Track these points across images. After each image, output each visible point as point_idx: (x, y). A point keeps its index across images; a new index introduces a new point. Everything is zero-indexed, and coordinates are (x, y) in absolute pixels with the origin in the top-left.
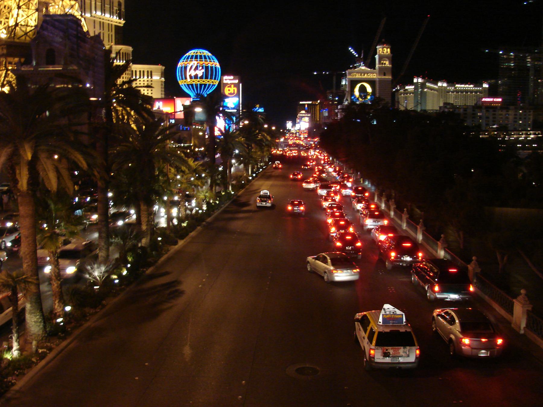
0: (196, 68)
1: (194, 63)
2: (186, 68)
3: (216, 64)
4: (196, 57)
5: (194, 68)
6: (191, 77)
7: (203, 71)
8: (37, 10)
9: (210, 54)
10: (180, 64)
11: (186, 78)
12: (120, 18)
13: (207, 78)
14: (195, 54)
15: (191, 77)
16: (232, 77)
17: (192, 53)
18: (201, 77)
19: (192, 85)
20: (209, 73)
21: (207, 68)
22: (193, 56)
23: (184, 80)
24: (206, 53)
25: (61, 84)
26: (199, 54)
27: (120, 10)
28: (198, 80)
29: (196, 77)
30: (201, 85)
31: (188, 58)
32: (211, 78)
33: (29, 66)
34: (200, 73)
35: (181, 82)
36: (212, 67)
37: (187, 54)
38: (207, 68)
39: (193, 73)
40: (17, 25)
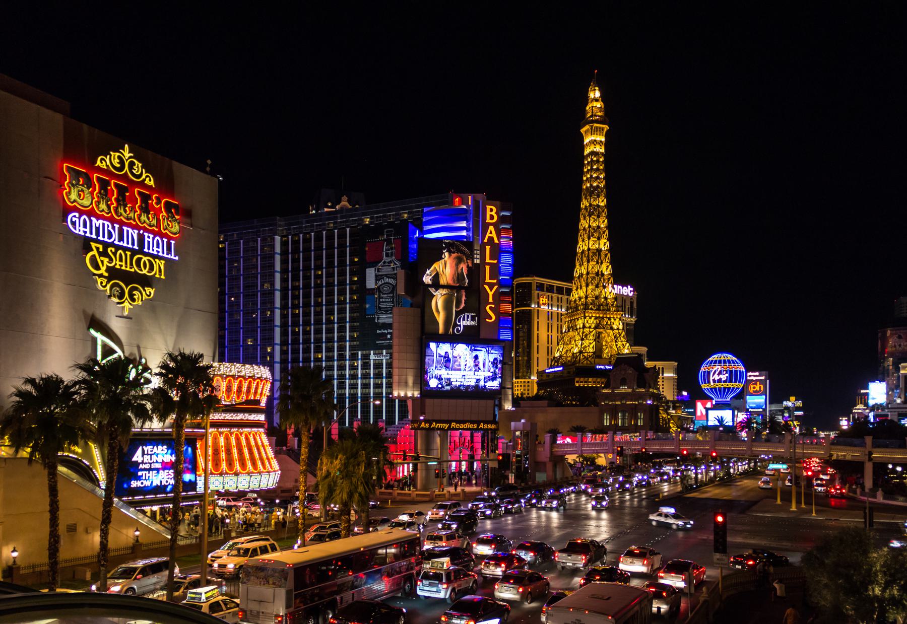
0: (720, 373)
1: (718, 368)
2: (709, 373)
4: (720, 362)
6: (714, 381)
9: (734, 358)
11: (709, 382)
12: (632, 316)
13: (731, 381)
15: (714, 381)
16: (757, 374)
17: (715, 357)
19: (715, 389)
20: (734, 376)
21: (731, 372)
24: (730, 357)
26: (722, 358)
29: (720, 381)
30: (724, 389)
32: (735, 382)
34: (724, 377)
35: (703, 386)
36: (736, 372)
37: (711, 359)
38: (731, 372)
39: (717, 377)
40: (581, 352)
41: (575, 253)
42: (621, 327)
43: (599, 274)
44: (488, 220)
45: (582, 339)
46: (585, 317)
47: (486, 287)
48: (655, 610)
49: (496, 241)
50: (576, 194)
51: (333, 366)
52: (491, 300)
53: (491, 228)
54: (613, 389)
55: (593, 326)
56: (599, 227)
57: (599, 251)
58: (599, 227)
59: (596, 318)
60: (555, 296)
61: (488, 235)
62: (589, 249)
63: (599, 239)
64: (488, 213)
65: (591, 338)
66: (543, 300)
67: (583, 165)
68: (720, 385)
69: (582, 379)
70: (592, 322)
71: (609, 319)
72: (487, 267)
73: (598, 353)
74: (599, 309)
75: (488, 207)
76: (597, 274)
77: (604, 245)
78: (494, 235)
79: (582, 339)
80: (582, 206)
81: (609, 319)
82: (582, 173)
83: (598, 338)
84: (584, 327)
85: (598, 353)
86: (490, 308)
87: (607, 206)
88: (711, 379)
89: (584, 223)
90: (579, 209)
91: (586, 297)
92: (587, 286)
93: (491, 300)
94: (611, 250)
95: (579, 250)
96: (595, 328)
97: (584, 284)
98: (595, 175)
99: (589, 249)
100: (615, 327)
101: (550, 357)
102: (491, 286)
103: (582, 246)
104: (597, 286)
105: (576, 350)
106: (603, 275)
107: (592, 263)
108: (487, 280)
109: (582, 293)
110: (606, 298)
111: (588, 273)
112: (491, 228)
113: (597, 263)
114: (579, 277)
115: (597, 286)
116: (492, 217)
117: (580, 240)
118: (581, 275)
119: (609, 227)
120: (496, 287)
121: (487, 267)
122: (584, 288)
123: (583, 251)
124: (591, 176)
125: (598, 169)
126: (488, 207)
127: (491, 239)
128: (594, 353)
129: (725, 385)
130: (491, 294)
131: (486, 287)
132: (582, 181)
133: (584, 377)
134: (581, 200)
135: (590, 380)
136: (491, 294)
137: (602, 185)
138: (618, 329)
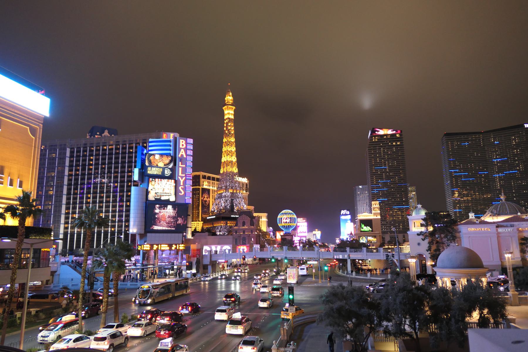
1: (285, 216)
3: (295, 216)
10: (279, 217)
17: (284, 211)
24: (290, 211)
27: (247, 187)
29: (286, 222)
34: (288, 221)
35: (279, 225)
38: (291, 218)
39: (285, 221)
44: (181, 146)
47: (180, 178)
48: (241, 250)
49: (185, 156)
51: (116, 205)
52: (182, 184)
53: (182, 150)
57: (232, 162)
60: (211, 181)
61: (181, 153)
63: (232, 156)
64: (181, 143)
68: (286, 225)
72: (180, 169)
75: (181, 141)
78: (184, 154)
80: (224, 141)
86: (182, 188)
89: (224, 149)
90: (223, 142)
93: (182, 184)
95: (223, 161)
102: (182, 177)
103: (224, 159)
107: (228, 167)
108: (180, 174)
112: (182, 150)
116: (183, 145)
117: (223, 156)
119: (236, 151)
120: (184, 178)
121: (180, 169)
126: (181, 141)
127: (182, 155)
129: (289, 224)
130: (182, 181)
131: (180, 178)
134: (223, 138)
136: (182, 181)
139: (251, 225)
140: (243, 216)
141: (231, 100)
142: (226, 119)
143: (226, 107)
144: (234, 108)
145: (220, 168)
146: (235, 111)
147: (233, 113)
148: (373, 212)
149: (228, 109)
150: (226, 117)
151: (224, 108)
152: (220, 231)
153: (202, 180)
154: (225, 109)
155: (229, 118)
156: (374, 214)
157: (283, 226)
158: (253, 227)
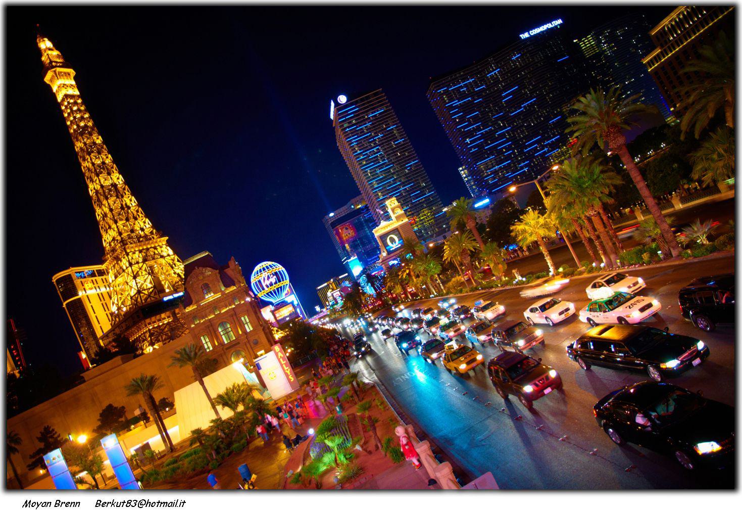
0: (268, 278)
1: (264, 275)
2: (260, 281)
4: (264, 269)
5: (266, 278)
6: (268, 287)
7: (275, 277)
8: (149, 274)
11: (263, 289)
13: (280, 281)
14: (261, 268)
17: (257, 268)
18: (276, 283)
19: (271, 292)
22: (260, 270)
23: (263, 291)
24: (270, 263)
25: (226, 307)
26: (264, 266)
28: (274, 285)
29: (271, 284)
30: (278, 289)
31: (257, 273)
33: (191, 306)
34: (273, 279)
38: (276, 274)
39: (268, 282)
40: (139, 292)
41: (90, 198)
42: (171, 252)
43: (125, 208)
45: (135, 277)
46: (127, 254)
50: (67, 140)
54: (197, 302)
55: (141, 260)
56: (103, 163)
57: (114, 185)
58: (103, 163)
59: (140, 251)
60: (99, 278)
62: (102, 186)
63: (109, 174)
65: (144, 273)
66: (88, 285)
67: (62, 112)
68: (275, 287)
69: (153, 319)
70: (138, 257)
71: (155, 248)
73: (158, 288)
74: (139, 241)
76: (122, 208)
77: (117, 178)
79: (135, 277)
81: (155, 248)
82: (64, 120)
83: (151, 272)
84: (131, 265)
85: (158, 288)
87: (104, 142)
88: (264, 285)
90: (76, 154)
91: (120, 234)
92: (116, 222)
94: (126, 182)
96: (145, 260)
97: (111, 222)
98: (78, 116)
99: (102, 186)
100: (165, 254)
101: (108, 312)
103: (92, 187)
104: (127, 220)
105: (133, 292)
106: (129, 208)
109: (113, 233)
110: (142, 230)
111: (111, 210)
113: (117, 197)
114: (104, 220)
115: (127, 220)
117: (88, 182)
118: (105, 215)
119: (115, 161)
122: (114, 226)
123: (97, 192)
124: (75, 118)
125: (79, 110)
128: (154, 287)
129: (277, 286)
132: (68, 127)
133: (155, 315)
135: (163, 316)
137: (90, 124)
138: (169, 255)
139: (227, 286)
140: (197, 270)
141: (58, 56)
142: (63, 100)
143: (50, 74)
144: (72, 72)
145: (94, 211)
146: (75, 78)
147: (73, 83)
148: (393, 216)
149: (57, 75)
150: (59, 99)
151: (47, 79)
152: (152, 344)
153: (77, 282)
154: (51, 81)
155: (67, 96)
156: (398, 218)
157: (270, 294)
158: (233, 288)
